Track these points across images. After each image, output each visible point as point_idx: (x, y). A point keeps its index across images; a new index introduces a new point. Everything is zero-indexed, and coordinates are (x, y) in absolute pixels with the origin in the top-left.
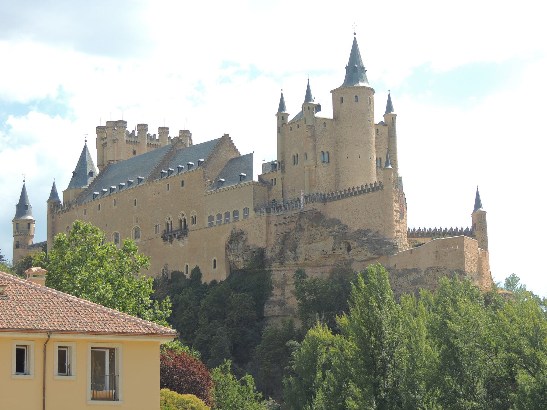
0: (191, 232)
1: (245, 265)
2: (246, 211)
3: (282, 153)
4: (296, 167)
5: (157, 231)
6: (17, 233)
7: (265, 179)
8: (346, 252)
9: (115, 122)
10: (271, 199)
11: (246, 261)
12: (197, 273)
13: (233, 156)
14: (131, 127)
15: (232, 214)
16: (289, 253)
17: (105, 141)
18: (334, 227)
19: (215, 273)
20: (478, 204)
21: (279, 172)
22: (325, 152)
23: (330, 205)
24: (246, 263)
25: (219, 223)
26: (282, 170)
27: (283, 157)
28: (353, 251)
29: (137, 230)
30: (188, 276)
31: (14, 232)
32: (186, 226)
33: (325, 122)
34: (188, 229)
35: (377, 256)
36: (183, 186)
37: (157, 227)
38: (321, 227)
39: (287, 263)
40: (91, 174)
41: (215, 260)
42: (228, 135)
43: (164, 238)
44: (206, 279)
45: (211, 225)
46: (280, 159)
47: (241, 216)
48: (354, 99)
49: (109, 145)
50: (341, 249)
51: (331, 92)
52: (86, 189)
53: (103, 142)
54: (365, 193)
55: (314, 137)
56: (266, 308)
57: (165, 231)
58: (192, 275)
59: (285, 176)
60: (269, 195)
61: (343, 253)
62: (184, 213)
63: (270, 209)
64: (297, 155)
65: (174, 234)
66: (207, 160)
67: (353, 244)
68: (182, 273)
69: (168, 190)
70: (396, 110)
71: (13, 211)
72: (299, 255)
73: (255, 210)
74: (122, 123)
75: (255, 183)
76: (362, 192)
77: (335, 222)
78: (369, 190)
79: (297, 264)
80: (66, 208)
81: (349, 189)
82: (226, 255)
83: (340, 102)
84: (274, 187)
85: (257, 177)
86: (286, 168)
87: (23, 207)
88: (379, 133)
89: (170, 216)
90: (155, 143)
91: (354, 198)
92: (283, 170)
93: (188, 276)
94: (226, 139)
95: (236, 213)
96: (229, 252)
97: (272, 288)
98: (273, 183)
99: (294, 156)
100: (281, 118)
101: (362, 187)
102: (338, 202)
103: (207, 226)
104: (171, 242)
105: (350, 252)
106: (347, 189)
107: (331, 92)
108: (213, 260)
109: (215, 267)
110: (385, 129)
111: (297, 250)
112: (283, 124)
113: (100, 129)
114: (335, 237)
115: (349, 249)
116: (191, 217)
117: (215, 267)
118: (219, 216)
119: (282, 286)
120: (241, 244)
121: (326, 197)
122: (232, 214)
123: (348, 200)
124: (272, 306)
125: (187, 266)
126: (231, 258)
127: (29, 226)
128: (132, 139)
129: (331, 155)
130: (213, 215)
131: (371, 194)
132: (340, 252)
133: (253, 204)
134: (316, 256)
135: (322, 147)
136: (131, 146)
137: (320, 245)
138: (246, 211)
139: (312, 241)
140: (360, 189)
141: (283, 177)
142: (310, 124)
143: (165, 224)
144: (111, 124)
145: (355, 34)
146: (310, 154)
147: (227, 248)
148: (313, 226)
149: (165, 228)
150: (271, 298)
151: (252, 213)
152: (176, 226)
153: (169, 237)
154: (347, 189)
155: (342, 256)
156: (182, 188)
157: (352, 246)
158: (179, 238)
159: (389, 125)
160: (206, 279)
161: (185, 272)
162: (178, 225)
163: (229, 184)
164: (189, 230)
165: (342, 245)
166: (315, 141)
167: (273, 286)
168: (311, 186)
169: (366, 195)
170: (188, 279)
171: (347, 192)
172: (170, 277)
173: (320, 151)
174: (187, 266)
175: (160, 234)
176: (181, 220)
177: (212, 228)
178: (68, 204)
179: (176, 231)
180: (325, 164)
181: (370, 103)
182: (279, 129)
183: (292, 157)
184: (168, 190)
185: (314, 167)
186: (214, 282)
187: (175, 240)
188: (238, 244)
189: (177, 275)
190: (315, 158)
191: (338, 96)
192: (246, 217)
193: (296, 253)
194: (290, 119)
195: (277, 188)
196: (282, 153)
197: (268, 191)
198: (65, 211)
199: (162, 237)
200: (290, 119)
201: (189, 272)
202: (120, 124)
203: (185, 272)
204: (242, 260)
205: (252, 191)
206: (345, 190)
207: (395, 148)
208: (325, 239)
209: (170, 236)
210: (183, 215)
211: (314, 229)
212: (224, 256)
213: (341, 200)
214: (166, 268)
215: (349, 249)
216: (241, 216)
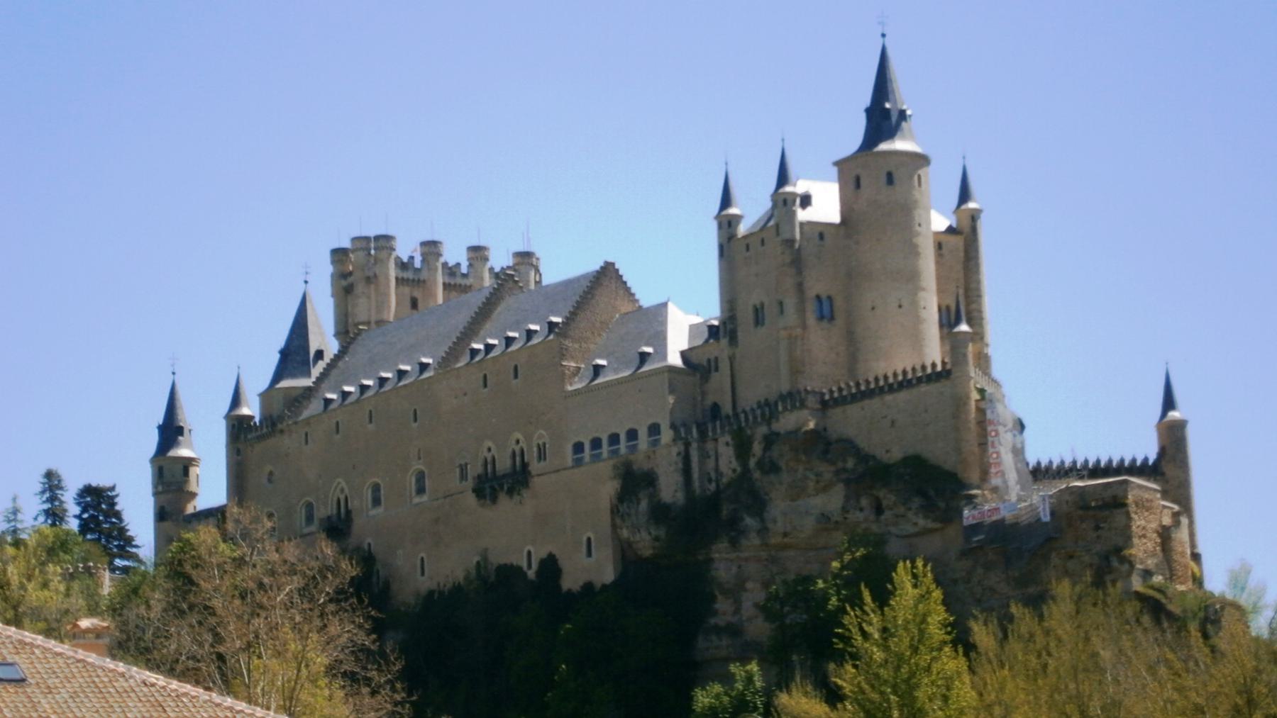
0: (535, 479)
1: (654, 548)
2: (654, 429)
4: (762, 331)
5: (463, 476)
6: (160, 488)
7: (694, 359)
8: (872, 517)
9: (367, 239)
10: (710, 401)
11: (657, 539)
12: (550, 567)
13: (626, 307)
14: (406, 248)
15: (623, 437)
17: (350, 279)
18: (845, 461)
19: (590, 566)
20: (1169, 402)
21: (724, 342)
22: (824, 297)
23: (836, 413)
24: (657, 544)
25: (596, 458)
28: (887, 515)
29: (421, 477)
30: (531, 574)
31: (155, 486)
32: (525, 466)
33: (820, 231)
34: (529, 473)
35: (938, 525)
36: (516, 376)
37: (463, 469)
39: (744, 542)
40: (320, 354)
41: (589, 539)
42: (613, 264)
43: (479, 492)
44: (571, 581)
45: (578, 463)
47: (643, 441)
48: (884, 178)
49: (360, 288)
50: (861, 510)
51: (837, 164)
52: (309, 389)
53: (344, 283)
55: (797, 262)
56: (701, 643)
57: (479, 477)
58: (538, 573)
60: (704, 394)
62: (520, 436)
63: (705, 424)
64: (762, 305)
65: (501, 483)
66: (567, 318)
67: (888, 498)
68: (519, 568)
69: (485, 386)
71: (153, 439)
72: (770, 526)
73: (673, 426)
74: (385, 242)
75: (672, 369)
76: (905, 383)
77: (849, 446)
78: (919, 380)
79: (767, 545)
80: (265, 430)
81: (877, 379)
82: (614, 526)
83: (852, 185)
85: (678, 355)
87: (171, 431)
88: (944, 251)
89: (490, 444)
90: (459, 281)
92: (733, 338)
93: (531, 574)
94: (608, 273)
95: (632, 435)
96: (618, 521)
97: (713, 599)
101: (905, 372)
103: (570, 462)
104: (494, 500)
105: (883, 517)
106: (871, 379)
107: (837, 164)
108: (585, 539)
109: (589, 554)
110: (958, 241)
111: (766, 514)
113: (339, 255)
114: (847, 482)
115: (879, 510)
116: (535, 444)
117: (589, 554)
118: (596, 443)
119: (735, 592)
121: (827, 397)
122: (623, 437)
123: (874, 404)
124: (714, 638)
125: (529, 553)
126: (625, 533)
127: (186, 472)
128: (409, 275)
129: (839, 303)
130: (582, 440)
131: (924, 388)
132: (860, 516)
134: (809, 524)
135: (817, 285)
136: (406, 290)
137: (818, 503)
138: (654, 429)
139: (797, 492)
140: (900, 378)
143: (480, 463)
144: (362, 242)
145: (883, 35)
146: (790, 303)
147: (614, 511)
149: (480, 470)
150: (713, 621)
151: (666, 435)
152: (504, 465)
153: (488, 491)
154: (871, 379)
155: (864, 526)
156: (514, 382)
157: (885, 503)
158: (510, 492)
159: (965, 235)
160: (571, 581)
161: (525, 565)
162: (509, 463)
163: (616, 371)
164: (533, 473)
165: (864, 502)
166: (799, 272)
167: (717, 593)
168: (795, 372)
169: (915, 391)
170: (532, 582)
171: (872, 386)
172: (493, 578)
174: (529, 553)
175: (470, 483)
176: (514, 453)
177: (583, 469)
178: (272, 422)
179: (504, 476)
180: (825, 324)
181: (920, 184)
182: (721, 248)
184: (485, 386)
185: (799, 331)
186: (588, 586)
187: (503, 498)
188: (638, 504)
189: (509, 573)
190: (801, 311)
191: (852, 174)
192: (655, 443)
193: (763, 520)
195: (720, 380)
198: (261, 438)
199: (474, 491)
201: (535, 566)
202: (382, 243)
203: (525, 565)
204: (648, 537)
206: (868, 382)
207: (978, 282)
208: (825, 489)
209: (492, 488)
210: (518, 442)
212: (608, 530)
213: (860, 404)
214: (485, 559)
215: (879, 510)
216: (643, 441)
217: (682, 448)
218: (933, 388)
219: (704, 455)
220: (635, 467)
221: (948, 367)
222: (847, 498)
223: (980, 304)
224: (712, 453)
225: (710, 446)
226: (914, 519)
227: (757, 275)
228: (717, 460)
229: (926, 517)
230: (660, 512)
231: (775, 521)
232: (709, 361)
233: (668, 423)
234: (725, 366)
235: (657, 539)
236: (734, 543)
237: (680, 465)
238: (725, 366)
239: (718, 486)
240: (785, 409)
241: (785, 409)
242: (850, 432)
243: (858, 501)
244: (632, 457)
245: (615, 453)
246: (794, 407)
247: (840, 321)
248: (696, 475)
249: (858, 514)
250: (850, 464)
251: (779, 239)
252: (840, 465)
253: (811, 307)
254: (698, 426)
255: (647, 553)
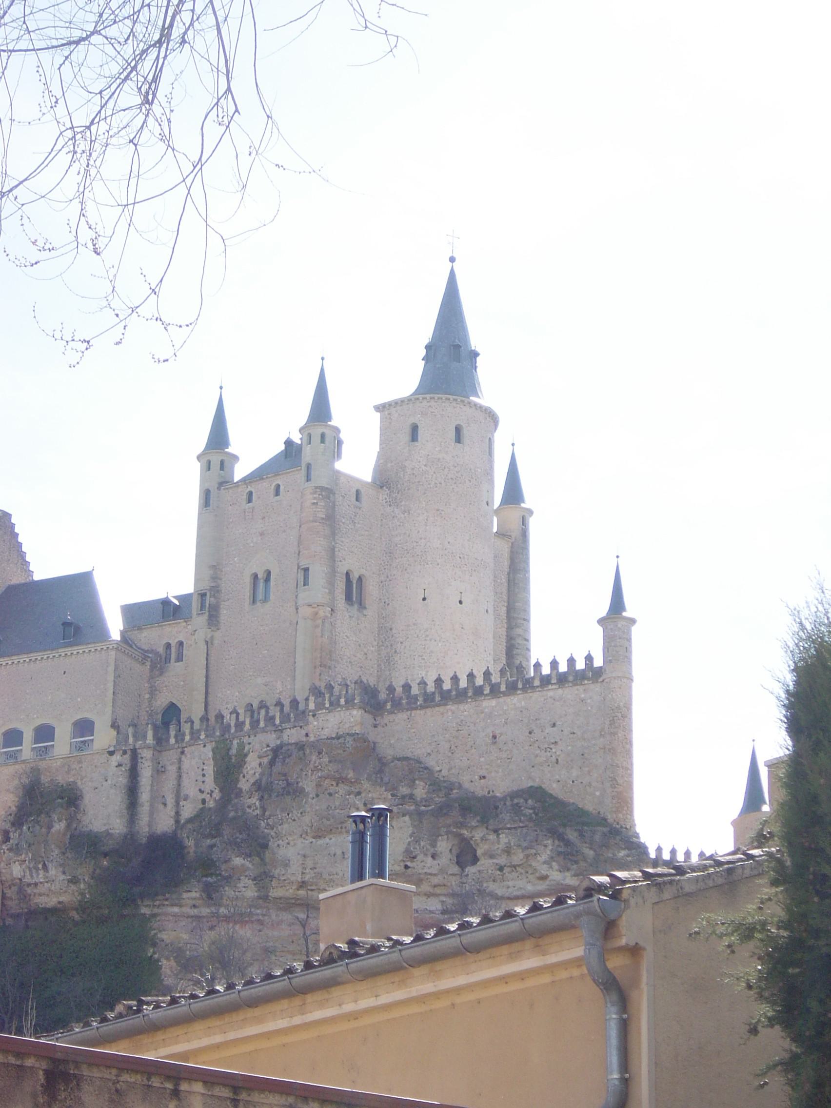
2: (84, 727)
3: (214, 567)
10: (161, 702)
16: (238, 861)
18: (412, 784)
26: (211, 617)
27: (215, 578)
28: (485, 863)
38: (366, 785)
46: (206, 585)
50: (433, 857)
54: (533, 687)
59: (217, 634)
61: (442, 871)
64: (269, 573)
70: (531, 498)
73: (114, 725)
77: (415, 768)
79: (265, 898)
84: (175, 668)
86: (224, 613)
91: (489, 704)
95: (45, 733)
98: (175, 652)
99: (255, 577)
100: (215, 465)
102: (429, 711)
105: (471, 870)
112: (221, 484)
120: (59, 826)
123: (466, 709)
131: (553, 692)
133: (109, 709)
138: (84, 727)
141: (212, 637)
142: (324, 482)
146: (318, 573)
148: (340, 780)
151: (103, 737)
155: (435, 880)
165: (444, 845)
169: (536, 696)
173: (342, 568)
183: (248, 580)
185: (325, 612)
192: (81, 747)
194: (240, 472)
196: (214, 567)
197: (151, 678)
200: (240, 472)
205: (111, 668)
211: (342, 789)
213: (441, 709)
216: (63, 742)
217: (127, 757)
218: (569, 693)
219: (159, 771)
220: (45, 779)
221: (598, 662)
222: (416, 839)
223: (527, 630)
224: (172, 769)
225: (169, 757)
226: (544, 870)
227: (262, 534)
228: (180, 777)
229: (564, 869)
230: (85, 844)
231: (286, 864)
232: (168, 646)
233: (107, 719)
234: (195, 654)
235: (74, 881)
236: (210, 893)
237: (123, 780)
238: (195, 654)
239: (177, 813)
240: (320, 706)
241: (320, 706)
242: (419, 750)
243: (434, 845)
244: (43, 765)
245: (13, 757)
246: (334, 704)
247: (371, 611)
248: (144, 796)
249: (430, 859)
250: (420, 791)
251: (309, 484)
252: (404, 790)
253: (341, 586)
254: (156, 728)
255: (51, 902)
